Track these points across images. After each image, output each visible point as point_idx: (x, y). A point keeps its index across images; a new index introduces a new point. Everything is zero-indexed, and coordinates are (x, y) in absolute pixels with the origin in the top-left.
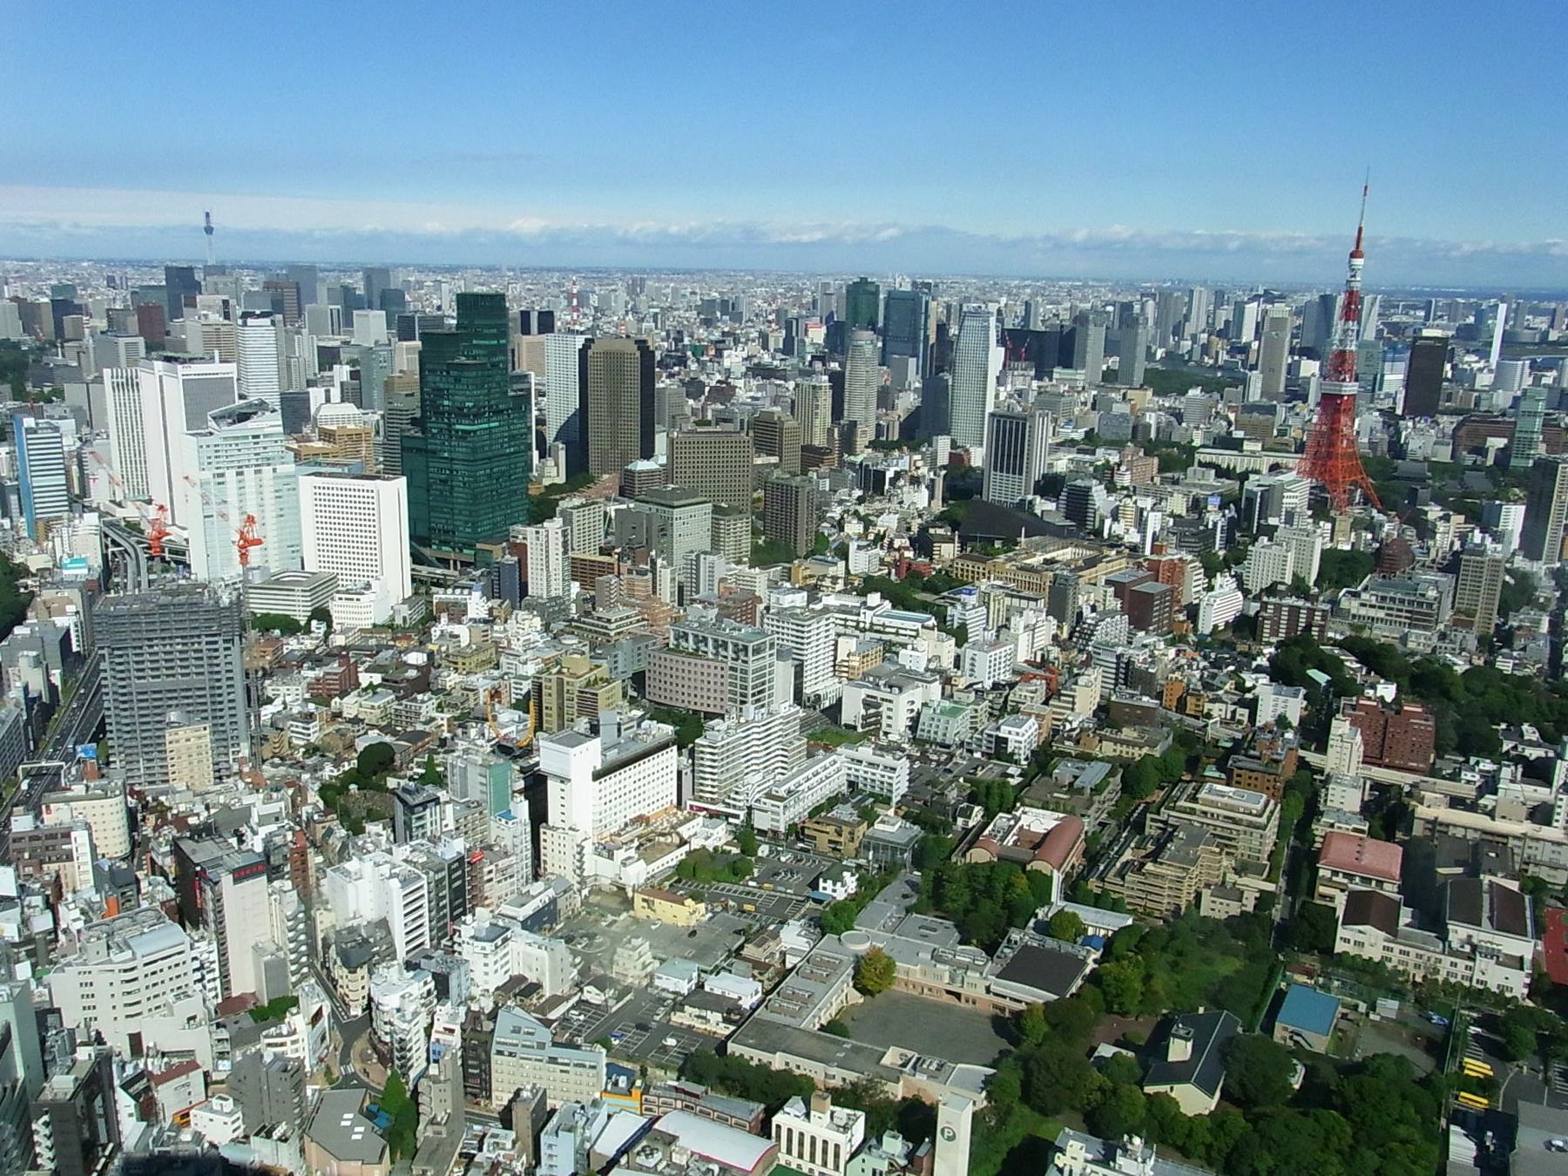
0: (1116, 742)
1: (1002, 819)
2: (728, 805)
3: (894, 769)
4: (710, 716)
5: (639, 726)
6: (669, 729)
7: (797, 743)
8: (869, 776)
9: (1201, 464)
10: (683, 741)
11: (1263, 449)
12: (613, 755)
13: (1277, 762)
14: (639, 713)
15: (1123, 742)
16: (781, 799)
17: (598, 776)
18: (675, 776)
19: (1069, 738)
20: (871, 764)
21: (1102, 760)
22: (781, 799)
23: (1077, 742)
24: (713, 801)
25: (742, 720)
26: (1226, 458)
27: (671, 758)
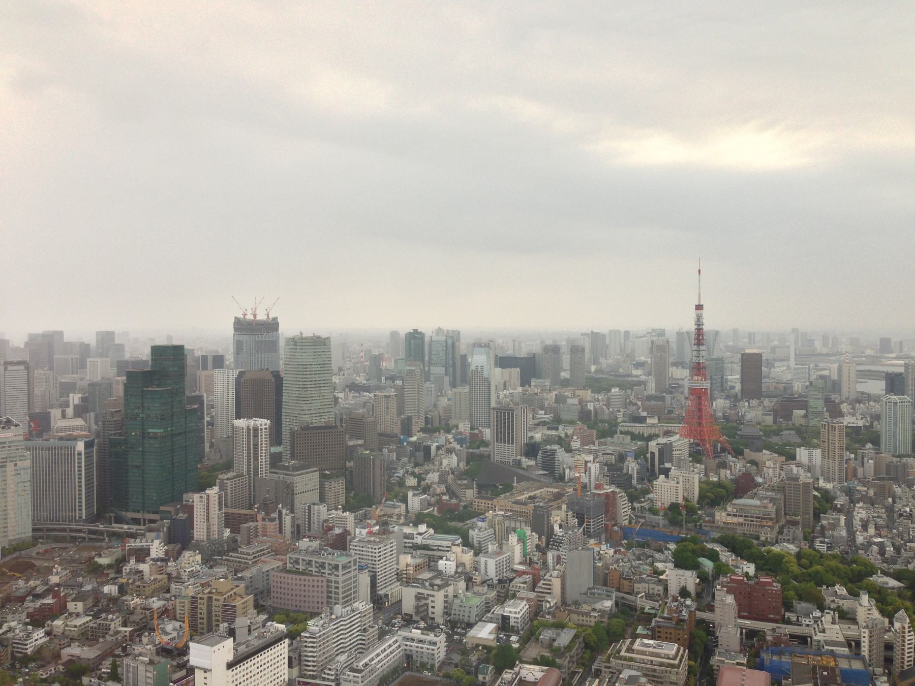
0: (579, 613)
1: (507, 676)
2: (324, 679)
3: (435, 644)
4: (313, 615)
5: (264, 626)
6: (282, 627)
7: (371, 630)
8: (419, 650)
9: (621, 433)
10: (292, 635)
12: (242, 649)
14: (263, 617)
15: (583, 614)
16: (359, 671)
17: (230, 666)
18: (286, 661)
19: (549, 613)
20: (421, 641)
22: (359, 671)
24: (313, 677)
25: (333, 617)
26: (638, 428)
27: (283, 649)
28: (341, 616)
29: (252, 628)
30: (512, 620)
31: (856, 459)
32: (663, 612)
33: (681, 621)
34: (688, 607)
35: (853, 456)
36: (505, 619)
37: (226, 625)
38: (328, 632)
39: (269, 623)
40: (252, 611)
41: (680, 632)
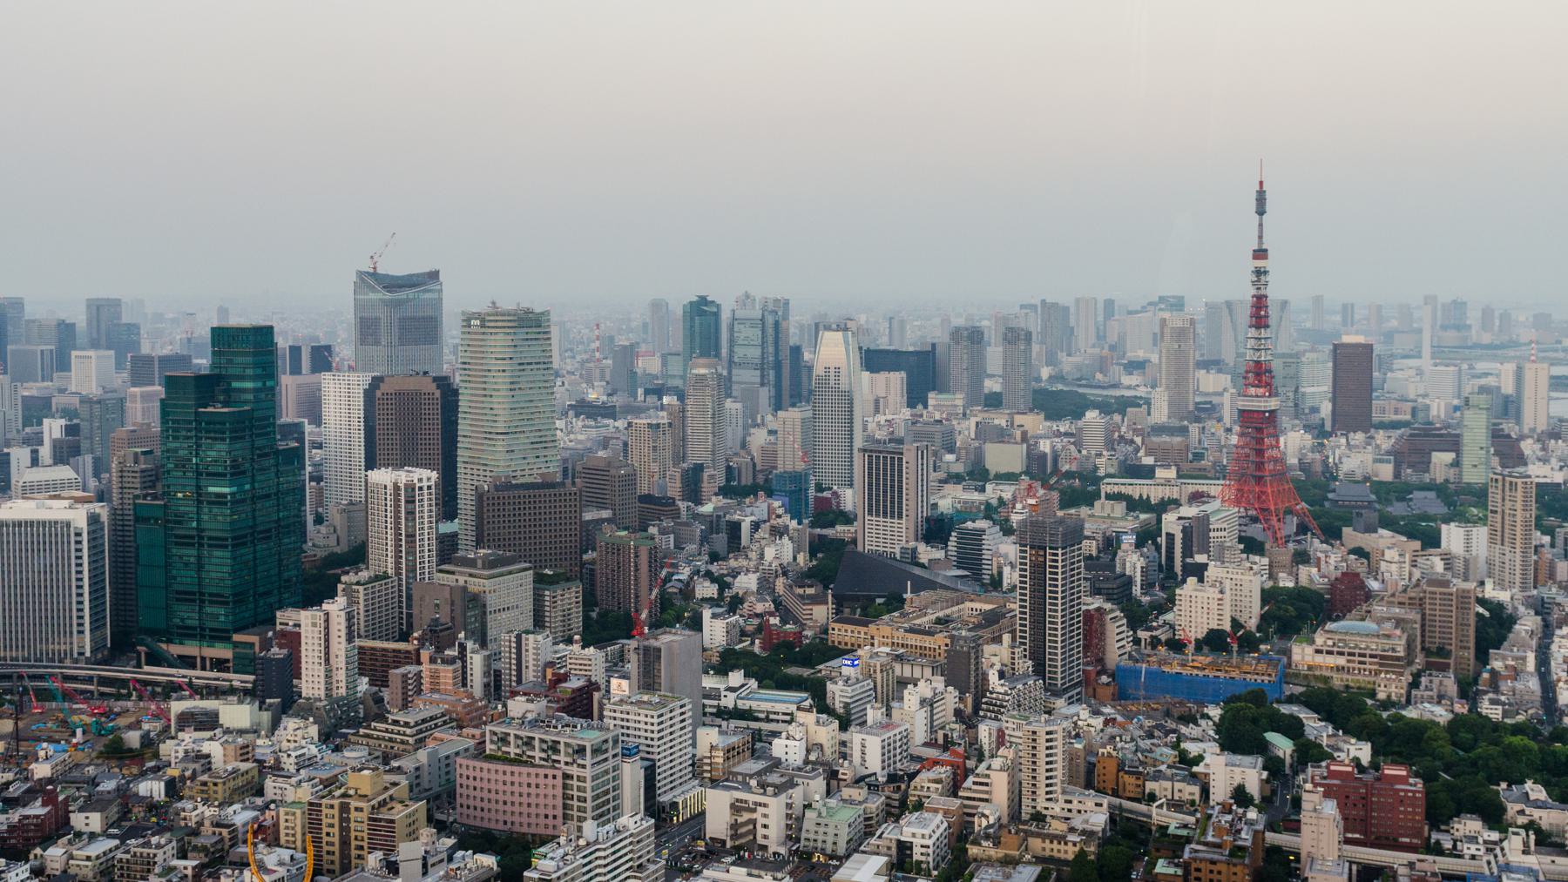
0: (1044, 837)
4: (544, 840)
5: (450, 859)
7: (652, 867)
9: (1109, 497)
11: (1179, 477)
13: (1241, 848)
14: (451, 842)
15: (1053, 838)
19: (987, 837)
21: (1029, 863)
23: (997, 844)
25: (582, 842)
26: (1137, 488)
28: (596, 842)
29: (431, 861)
30: (917, 851)
31: (1553, 545)
32: (1204, 833)
33: (1238, 851)
34: (1250, 823)
35: (1547, 539)
36: (904, 848)
37: (379, 854)
38: (573, 871)
39: (460, 854)
40: (427, 833)
41: (1238, 869)
